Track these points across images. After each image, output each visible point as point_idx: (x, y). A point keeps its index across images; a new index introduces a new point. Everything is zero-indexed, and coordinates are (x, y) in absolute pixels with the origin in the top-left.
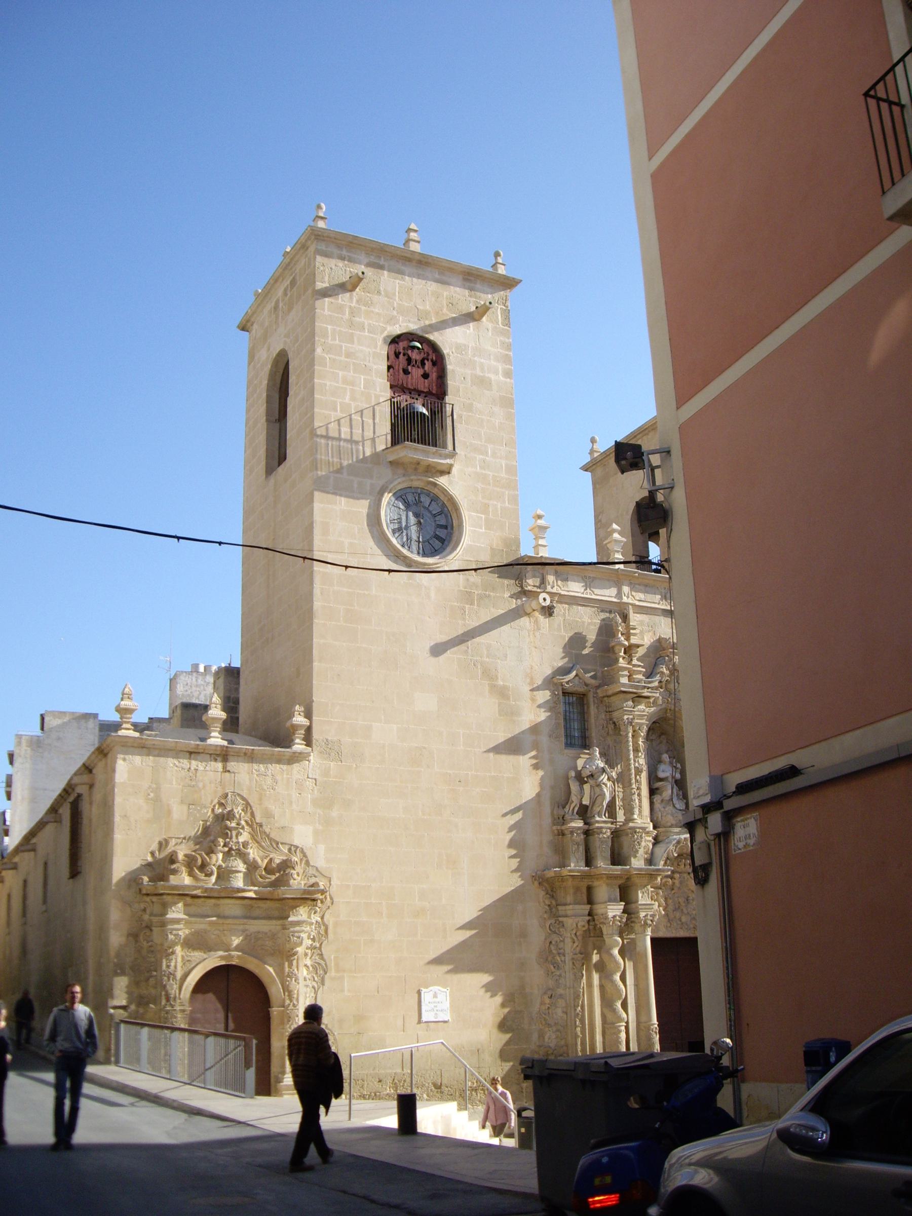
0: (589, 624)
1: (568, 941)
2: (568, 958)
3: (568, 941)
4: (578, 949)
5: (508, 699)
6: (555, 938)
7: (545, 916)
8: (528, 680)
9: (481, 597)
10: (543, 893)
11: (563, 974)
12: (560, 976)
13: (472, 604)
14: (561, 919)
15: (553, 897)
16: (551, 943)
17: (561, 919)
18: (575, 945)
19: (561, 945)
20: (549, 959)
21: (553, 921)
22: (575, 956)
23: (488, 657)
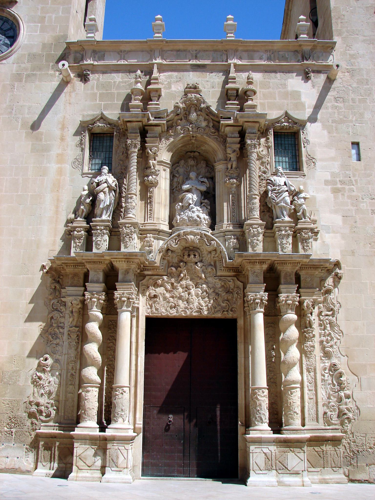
0: (120, 82)
1: (67, 316)
2: (66, 331)
3: (67, 316)
4: (74, 323)
5: (41, 140)
6: (56, 314)
7: (50, 297)
8: (60, 126)
9: (28, 76)
10: (50, 279)
11: (61, 343)
12: (57, 344)
13: (21, 81)
14: (63, 299)
15: (58, 282)
16: (52, 318)
17: (63, 299)
18: (71, 319)
19: (62, 320)
20: (49, 330)
21: (55, 301)
22: (71, 329)
23: (28, 114)
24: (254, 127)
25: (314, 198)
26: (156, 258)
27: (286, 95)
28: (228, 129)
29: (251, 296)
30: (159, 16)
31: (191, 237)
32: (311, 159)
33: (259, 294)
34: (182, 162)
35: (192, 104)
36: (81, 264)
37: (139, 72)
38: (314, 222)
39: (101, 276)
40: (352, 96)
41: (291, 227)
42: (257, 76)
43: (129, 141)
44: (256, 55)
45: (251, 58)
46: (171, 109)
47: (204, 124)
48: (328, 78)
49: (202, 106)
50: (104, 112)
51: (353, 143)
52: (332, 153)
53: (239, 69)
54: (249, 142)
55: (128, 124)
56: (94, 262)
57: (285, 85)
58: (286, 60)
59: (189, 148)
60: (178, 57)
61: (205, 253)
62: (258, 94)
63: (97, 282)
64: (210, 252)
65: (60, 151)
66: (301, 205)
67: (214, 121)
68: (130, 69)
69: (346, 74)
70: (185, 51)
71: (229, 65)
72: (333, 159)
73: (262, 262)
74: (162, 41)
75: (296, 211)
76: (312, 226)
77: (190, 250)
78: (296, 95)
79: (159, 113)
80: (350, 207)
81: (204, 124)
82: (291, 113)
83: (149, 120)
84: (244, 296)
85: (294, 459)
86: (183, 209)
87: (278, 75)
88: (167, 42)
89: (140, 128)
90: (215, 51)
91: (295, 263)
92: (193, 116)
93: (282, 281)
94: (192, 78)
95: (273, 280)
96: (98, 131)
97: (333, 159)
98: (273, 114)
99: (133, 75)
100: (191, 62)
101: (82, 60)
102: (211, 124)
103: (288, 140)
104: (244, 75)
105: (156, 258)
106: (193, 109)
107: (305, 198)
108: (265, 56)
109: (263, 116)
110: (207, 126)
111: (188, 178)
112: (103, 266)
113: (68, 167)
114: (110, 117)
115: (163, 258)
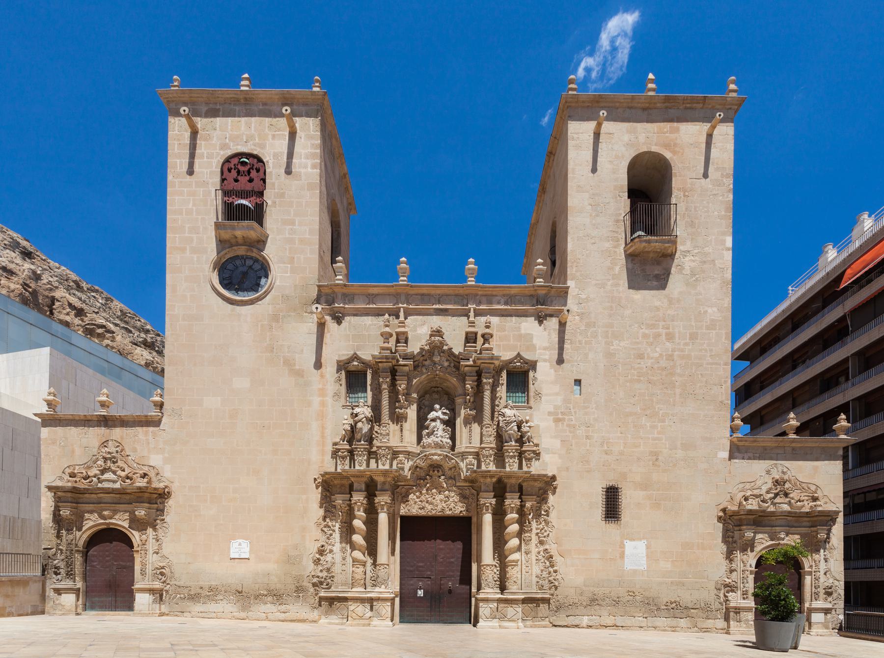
24: (489, 368)
25: (538, 426)
26: (407, 473)
27: (520, 337)
28: (466, 368)
29: (482, 501)
30: (403, 259)
31: (436, 457)
32: (538, 394)
33: (489, 500)
34: (427, 396)
35: (436, 346)
36: (347, 478)
37: (387, 316)
38: (537, 445)
39: (363, 487)
40: (580, 338)
41: (516, 450)
42: (495, 320)
43: (381, 380)
44: (495, 299)
45: (490, 302)
46: (416, 351)
47: (446, 364)
48: (560, 322)
49: (445, 348)
50: (358, 353)
51: (576, 381)
52: (556, 388)
53: (478, 313)
54: (485, 381)
55: (380, 364)
56: (357, 476)
57: (519, 328)
58: (522, 304)
59: (434, 384)
60: (423, 302)
61: (446, 469)
62: (494, 337)
63: (360, 491)
64: (451, 469)
65: (321, 386)
66: (526, 432)
67: (455, 360)
68: (379, 313)
69: (577, 317)
70: (429, 295)
71: (470, 309)
72: (557, 394)
73: (492, 477)
74: (407, 285)
75: (522, 437)
76: (535, 448)
77: (435, 467)
78: (529, 337)
79: (406, 355)
80: (568, 433)
81: (446, 364)
82: (521, 353)
83: (398, 361)
84: (478, 501)
85: (510, 611)
86: (429, 435)
87: (514, 318)
88: (411, 286)
89: (390, 368)
90: (456, 295)
91: (518, 478)
92: (437, 359)
93: (508, 490)
94: (436, 321)
95: (500, 489)
96: (353, 369)
97: (557, 394)
98: (507, 356)
99: (381, 318)
100: (434, 306)
101: (333, 302)
102: (452, 365)
103: (519, 377)
104: (482, 320)
105: (407, 473)
106: (436, 353)
107: (530, 427)
108: (502, 301)
109: (498, 358)
110: (449, 366)
111: (433, 409)
112: (365, 479)
113: (329, 400)
114: (363, 357)
115: (412, 473)
